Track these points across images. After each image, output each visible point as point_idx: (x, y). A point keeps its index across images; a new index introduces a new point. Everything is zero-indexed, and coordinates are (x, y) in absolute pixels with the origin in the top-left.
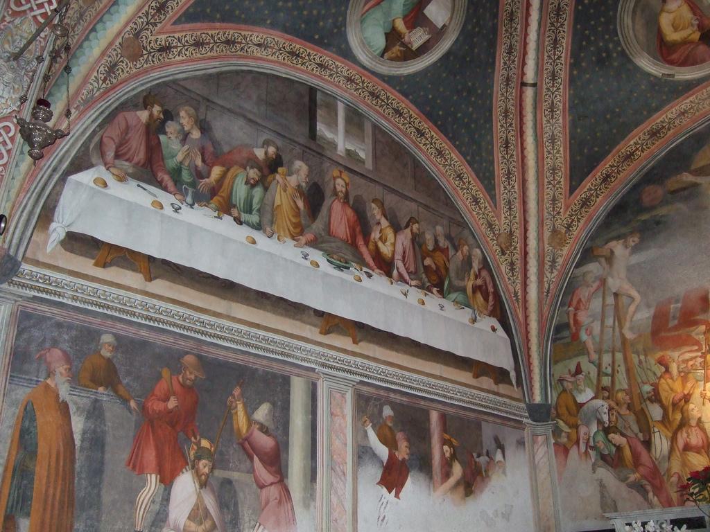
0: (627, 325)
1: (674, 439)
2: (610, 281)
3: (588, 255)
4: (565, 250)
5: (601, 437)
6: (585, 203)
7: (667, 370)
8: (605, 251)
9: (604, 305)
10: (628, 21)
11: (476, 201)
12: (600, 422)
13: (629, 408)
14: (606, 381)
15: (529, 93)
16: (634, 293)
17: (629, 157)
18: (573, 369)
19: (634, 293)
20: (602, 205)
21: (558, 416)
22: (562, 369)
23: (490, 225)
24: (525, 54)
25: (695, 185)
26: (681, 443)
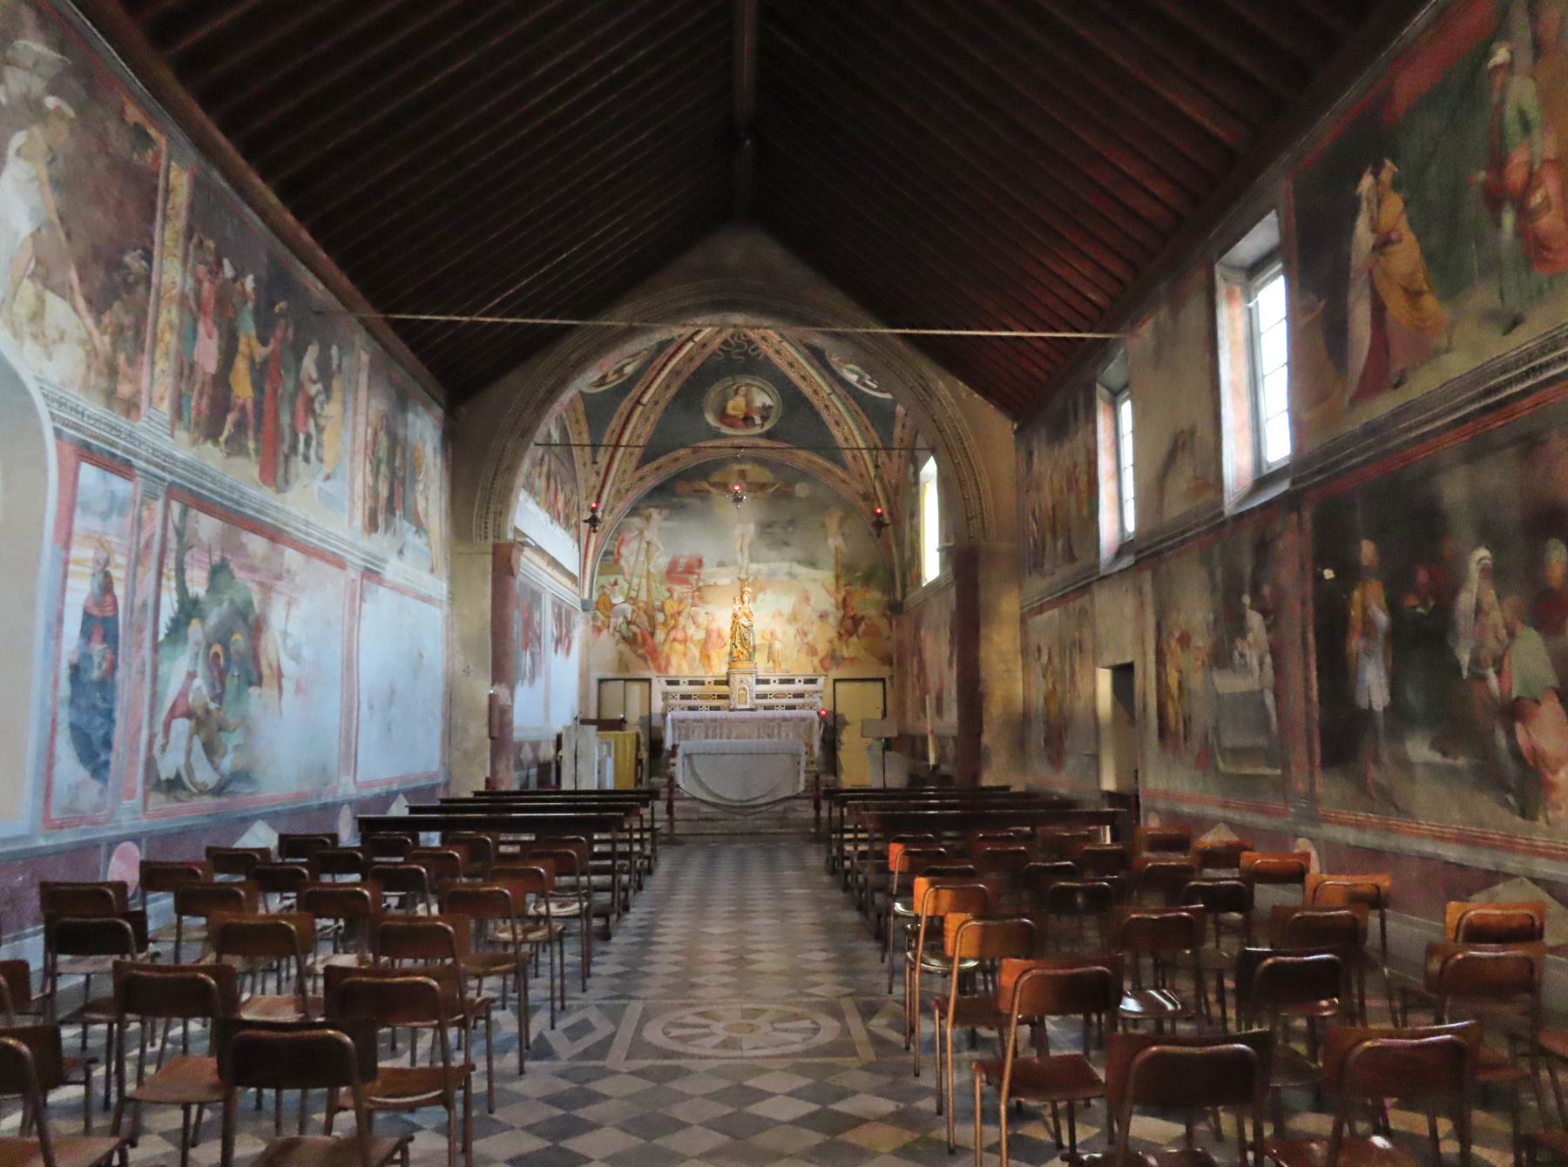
0: (652, 563)
1: (668, 634)
2: (646, 532)
3: (634, 511)
4: (621, 505)
5: (624, 626)
6: (641, 479)
7: (671, 596)
8: (646, 512)
9: (639, 548)
10: (713, 395)
11: (585, 464)
12: (625, 617)
13: (645, 612)
14: (633, 594)
15: (640, 408)
16: (661, 546)
17: (676, 460)
18: (612, 581)
19: (661, 546)
20: (651, 482)
21: (598, 609)
22: (604, 580)
23: (586, 481)
24: (648, 387)
25: (709, 492)
26: (671, 637)
